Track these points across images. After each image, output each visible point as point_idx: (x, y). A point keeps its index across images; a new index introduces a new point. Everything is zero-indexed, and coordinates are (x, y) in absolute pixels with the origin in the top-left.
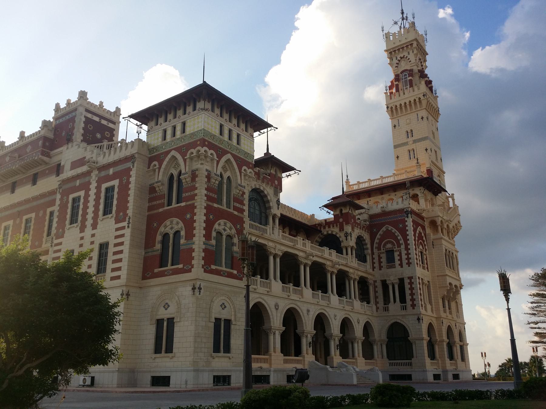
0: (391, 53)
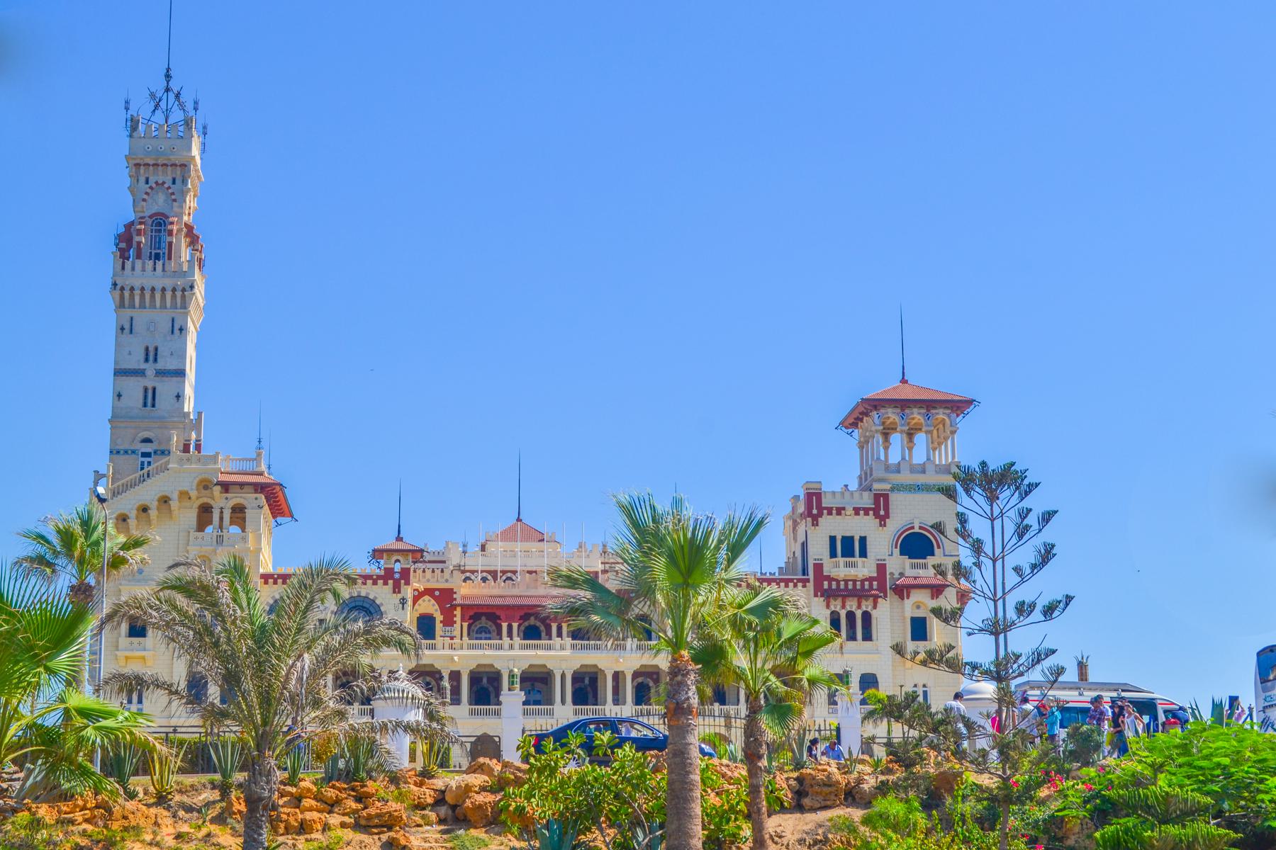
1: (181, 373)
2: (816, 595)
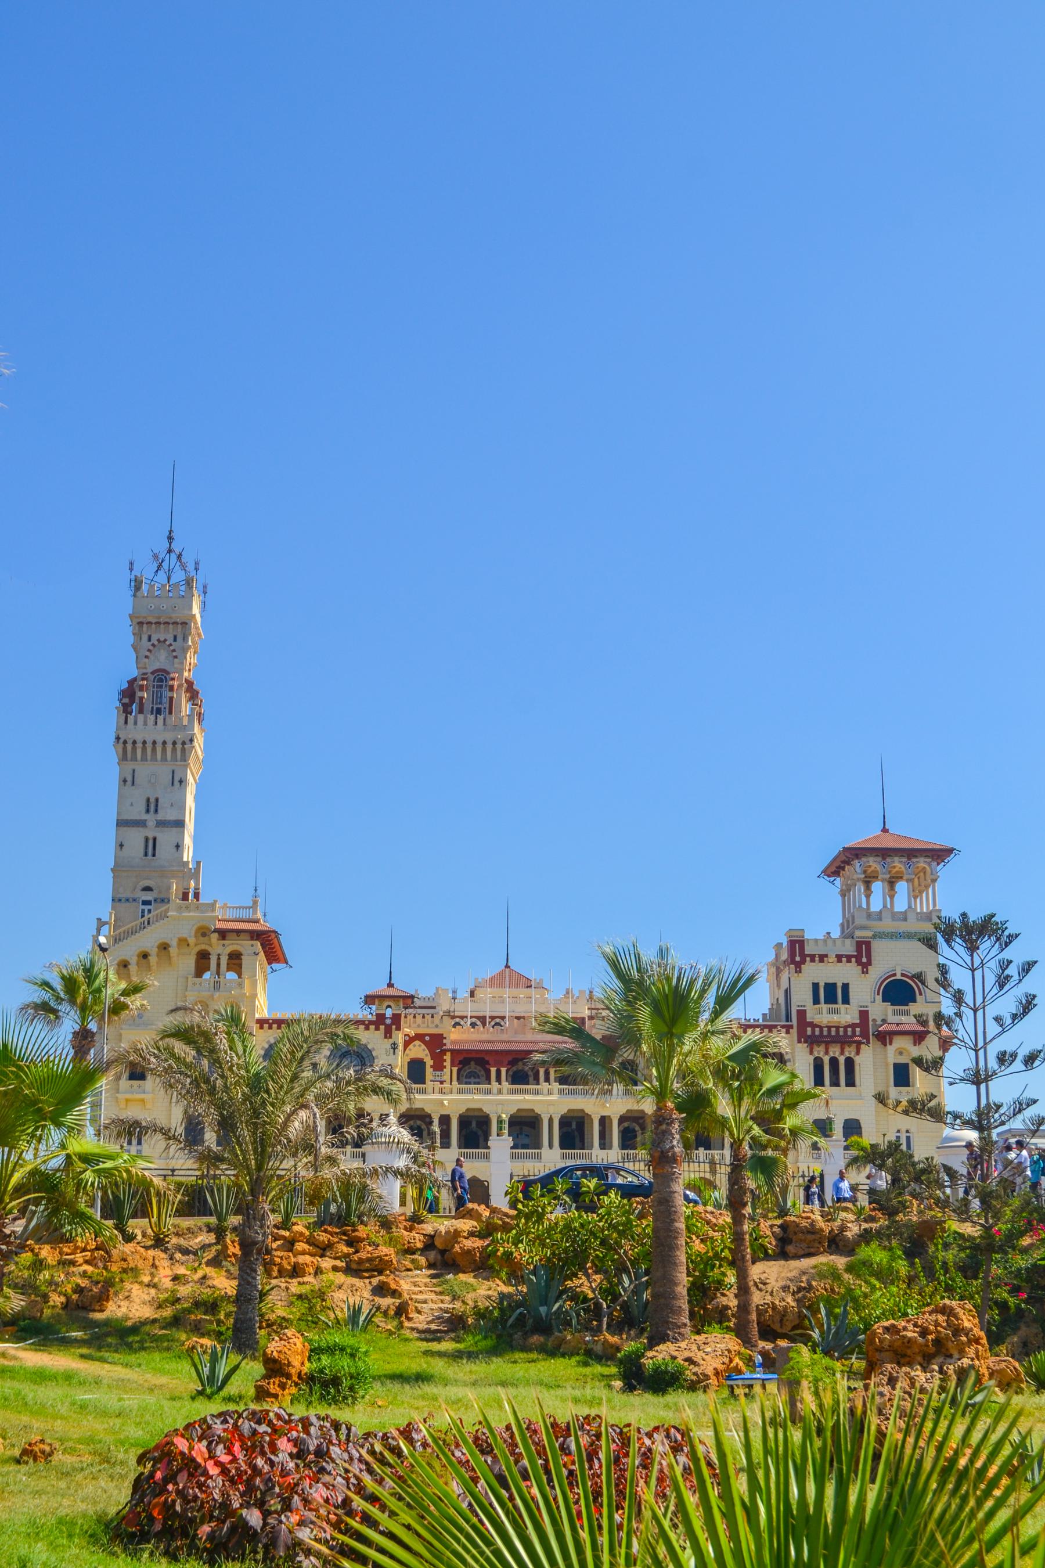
1: (180, 824)
2: (799, 1041)
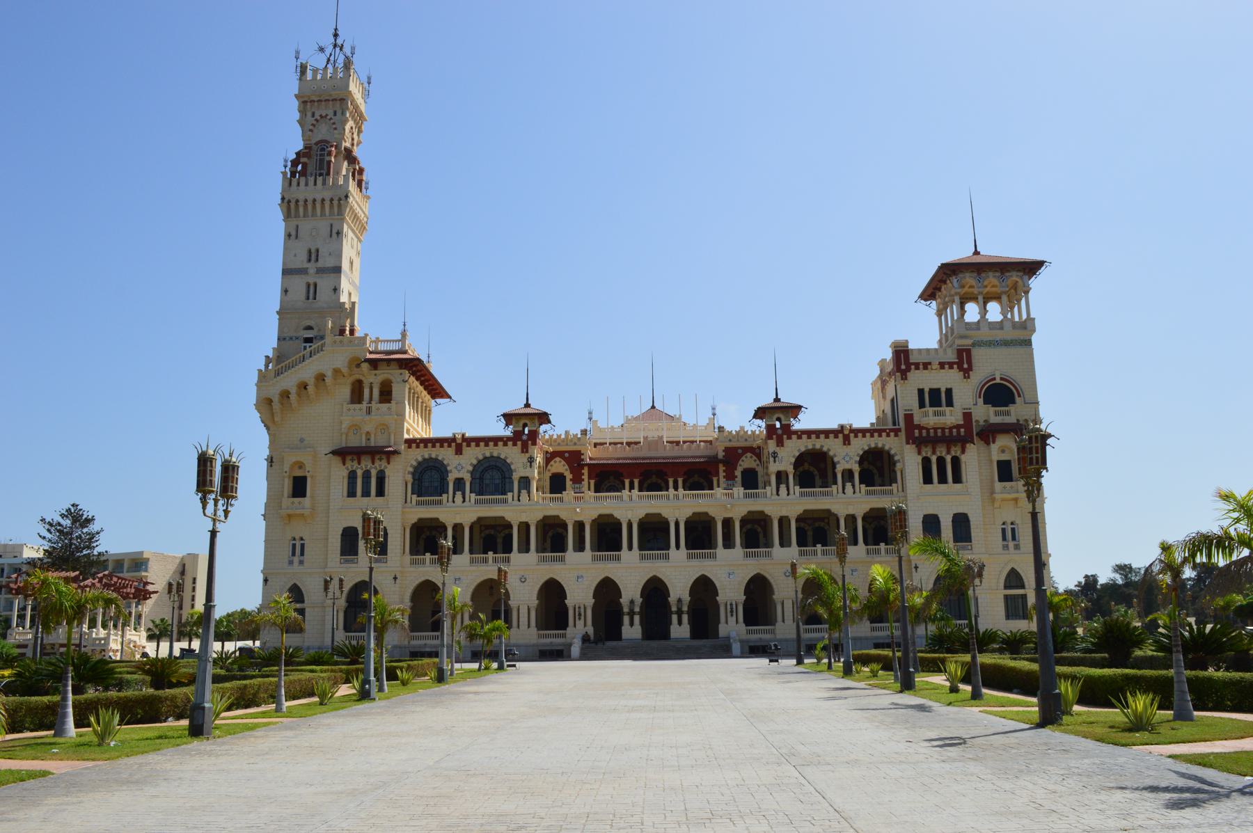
0: (305, 102)
1: (337, 270)
